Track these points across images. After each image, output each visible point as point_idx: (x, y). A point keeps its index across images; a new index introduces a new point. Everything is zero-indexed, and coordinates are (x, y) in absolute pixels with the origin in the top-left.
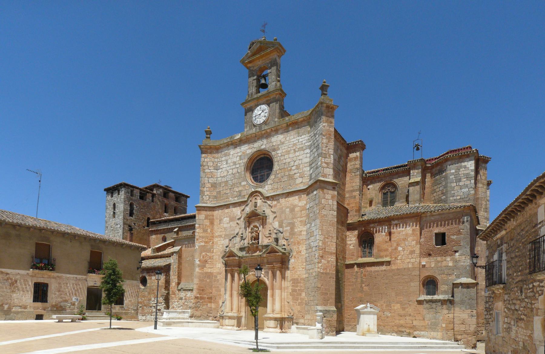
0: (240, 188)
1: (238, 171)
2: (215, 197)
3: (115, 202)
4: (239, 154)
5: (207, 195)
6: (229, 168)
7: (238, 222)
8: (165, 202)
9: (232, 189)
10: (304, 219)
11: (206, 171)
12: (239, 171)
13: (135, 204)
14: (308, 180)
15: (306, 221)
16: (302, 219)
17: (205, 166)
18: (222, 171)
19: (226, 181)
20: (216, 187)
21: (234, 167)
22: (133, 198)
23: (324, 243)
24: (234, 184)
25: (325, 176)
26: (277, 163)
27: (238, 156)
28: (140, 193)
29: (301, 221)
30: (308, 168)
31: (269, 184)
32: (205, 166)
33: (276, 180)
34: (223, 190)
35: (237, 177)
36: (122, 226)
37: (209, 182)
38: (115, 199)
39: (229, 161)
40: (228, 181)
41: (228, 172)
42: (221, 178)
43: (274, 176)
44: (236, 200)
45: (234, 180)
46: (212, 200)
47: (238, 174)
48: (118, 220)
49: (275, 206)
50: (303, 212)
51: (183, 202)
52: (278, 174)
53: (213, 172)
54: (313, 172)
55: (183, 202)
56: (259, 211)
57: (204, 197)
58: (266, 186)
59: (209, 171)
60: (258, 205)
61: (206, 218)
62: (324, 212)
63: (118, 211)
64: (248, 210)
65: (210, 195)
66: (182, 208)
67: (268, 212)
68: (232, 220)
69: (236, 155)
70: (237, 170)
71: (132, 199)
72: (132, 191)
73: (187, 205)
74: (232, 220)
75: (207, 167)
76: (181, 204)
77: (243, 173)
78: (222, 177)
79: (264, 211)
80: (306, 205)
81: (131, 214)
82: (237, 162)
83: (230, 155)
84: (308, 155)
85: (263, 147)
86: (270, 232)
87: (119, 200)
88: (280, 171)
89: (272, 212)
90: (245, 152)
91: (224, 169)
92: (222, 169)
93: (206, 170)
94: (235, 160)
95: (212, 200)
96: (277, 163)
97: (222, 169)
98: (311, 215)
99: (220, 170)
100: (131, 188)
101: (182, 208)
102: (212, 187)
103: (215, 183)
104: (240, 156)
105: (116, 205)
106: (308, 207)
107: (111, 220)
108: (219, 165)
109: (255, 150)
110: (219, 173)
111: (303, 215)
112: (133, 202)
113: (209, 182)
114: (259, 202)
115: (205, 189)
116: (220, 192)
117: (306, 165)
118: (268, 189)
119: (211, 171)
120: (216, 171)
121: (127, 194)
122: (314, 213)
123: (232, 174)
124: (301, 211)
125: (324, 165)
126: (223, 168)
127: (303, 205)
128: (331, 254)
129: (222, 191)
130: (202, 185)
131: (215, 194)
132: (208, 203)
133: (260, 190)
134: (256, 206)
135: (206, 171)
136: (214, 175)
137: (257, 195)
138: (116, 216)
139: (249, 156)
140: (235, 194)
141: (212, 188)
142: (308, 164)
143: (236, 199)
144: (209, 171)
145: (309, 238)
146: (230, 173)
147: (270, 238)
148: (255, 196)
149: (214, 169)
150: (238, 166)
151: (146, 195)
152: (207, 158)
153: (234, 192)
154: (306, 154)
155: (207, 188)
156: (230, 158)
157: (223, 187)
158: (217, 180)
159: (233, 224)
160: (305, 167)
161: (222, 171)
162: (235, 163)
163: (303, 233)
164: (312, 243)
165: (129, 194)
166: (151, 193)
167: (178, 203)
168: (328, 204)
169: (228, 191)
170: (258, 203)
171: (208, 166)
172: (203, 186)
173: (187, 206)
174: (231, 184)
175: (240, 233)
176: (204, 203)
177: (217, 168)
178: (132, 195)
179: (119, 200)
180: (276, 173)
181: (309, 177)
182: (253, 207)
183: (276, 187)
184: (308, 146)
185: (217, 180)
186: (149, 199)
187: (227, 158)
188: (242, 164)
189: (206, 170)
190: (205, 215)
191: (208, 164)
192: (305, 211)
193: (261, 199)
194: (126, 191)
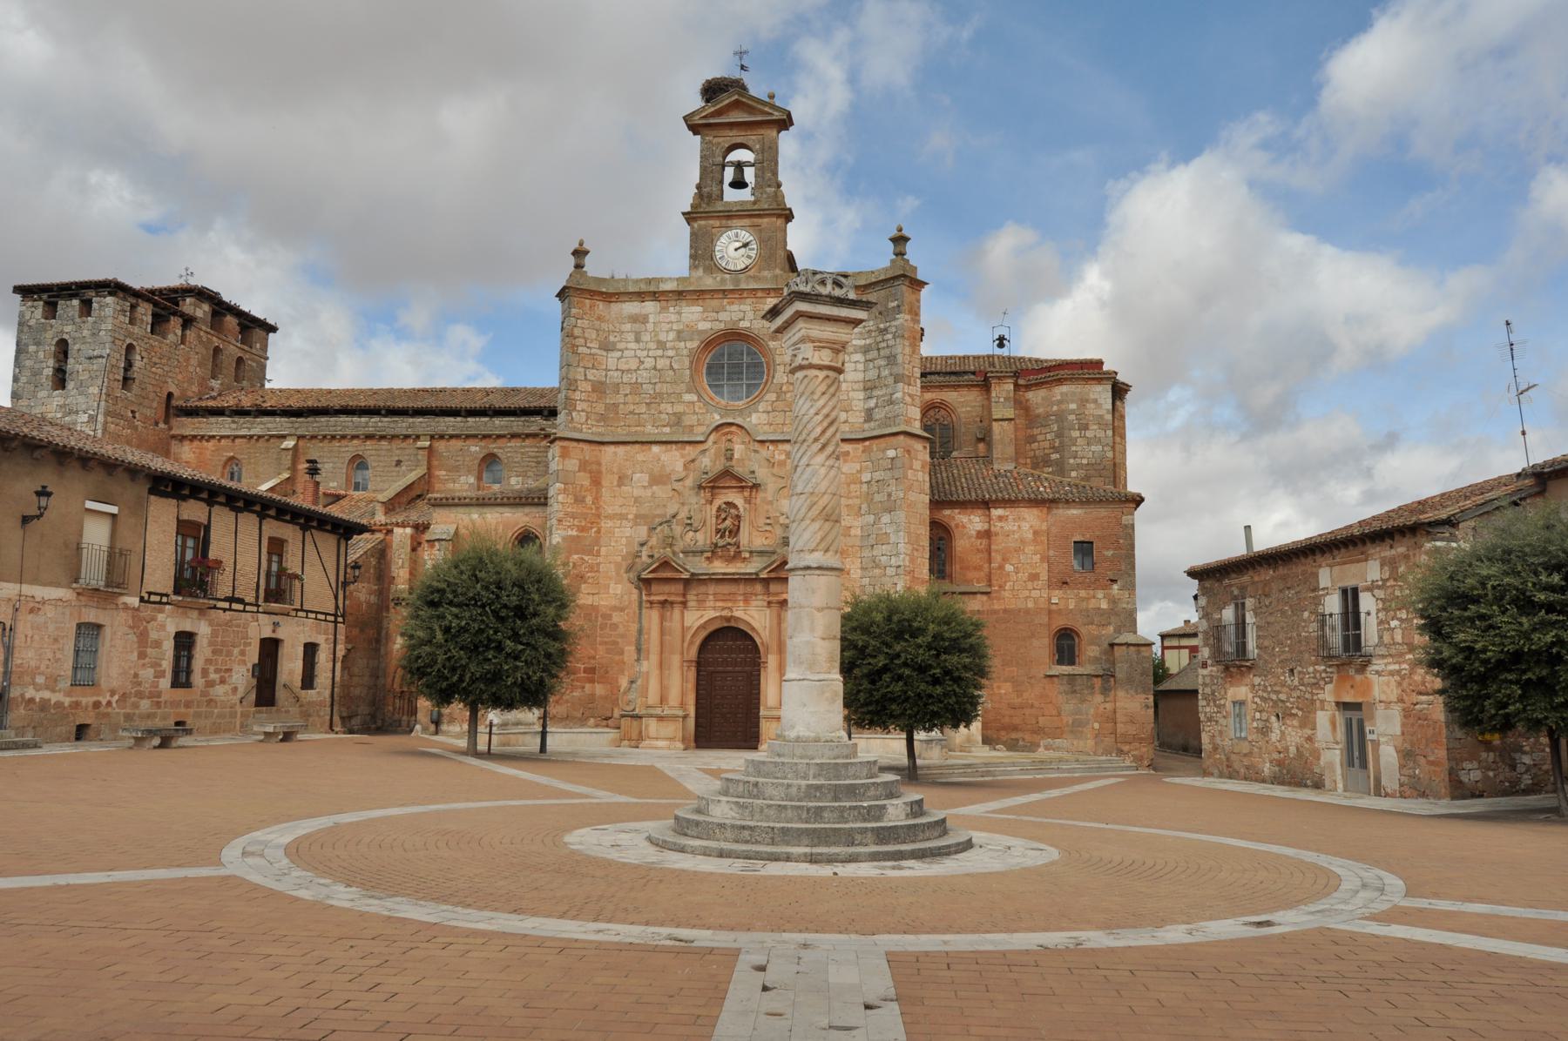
0: (679, 408)
1: (671, 366)
2: (602, 418)
3: (66, 337)
4: (674, 328)
5: (583, 411)
6: (645, 353)
7: (677, 486)
8: (213, 342)
9: (653, 405)
10: (857, 501)
11: (581, 350)
12: (675, 366)
13: (137, 348)
14: (862, 420)
15: (860, 508)
16: (850, 502)
17: (578, 337)
18: (622, 357)
19: (636, 383)
20: (605, 392)
21: (660, 352)
22: (136, 330)
23: (912, 560)
24: (660, 394)
25: (908, 422)
26: (782, 367)
27: (672, 330)
28: (154, 315)
29: (847, 506)
30: (861, 395)
31: (761, 410)
32: (578, 337)
33: (780, 405)
34: (624, 404)
35: (668, 379)
36: (101, 418)
37: (586, 379)
38: (68, 329)
39: (646, 337)
40: (642, 384)
41: (643, 363)
42: (619, 373)
43: (775, 395)
44: (666, 432)
45: (658, 387)
46: (594, 423)
47: (671, 373)
48: (81, 399)
49: (782, 464)
50: (852, 486)
51: (258, 345)
52: (785, 393)
53: (596, 354)
54: (876, 406)
55: (258, 345)
56: (739, 470)
57: (574, 414)
58: (754, 416)
59: (588, 351)
60: (736, 456)
61: (584, 466)
62: (913, 496)
63: (80, 368)
64: (709, 462)
65: (589, 410)
66: (254, 364)
67: (762, 474)
68: (658, 479)
69: (666, 327)
70: (668, 363)
71: (130, 335)
72: (133, 307)
73: (269, 354)
74: (658, 479)
75: (581, 341)
76: (254, 351)
77: (688, 372)
78: (623, 372)
79: (753, 472)
80: (860, 472)
81: (127, 381)
82: (669, 345)
83: (648, 322)
84: (860, 367)
85: (744, 324)
86: (768, 521)
87: (86, 333)
88: (791, 388)
89: (774, 475)
90: (692, 324)
91: (626, 353)
92: (622, 351)
93: (580, 349)
94: (662, 337)
95: (594, 423)
96: (782, 367)
97: (622, 351)
98: (877, 498)
99: (619, 354)
100: (134, 301)
101: (254, 364)
102: (594, 390)
103: (602, 383)
104: (679, 332)
105: (73, 348)
106: (866, 477)
107: (42, 394)
108: (612, 338)
109: (722, 326)
110: (612, 359)
111: (853, 494)
112: (134, 343)
113: (586, 379)
114: (739, 450)
115: (577, 395)
116: (616, 405)
117: (856, 386)
118: (759, 422)
119: (593, 351)
120: (605, 353)
121: (122, 318)
122: (889, 495)
123: (655, 368)
124: (849, 485)
125: (908, 399)
126: (627, 349)
127: (855, 472)
128: (923, 582)
129: (621, 406)
130: (570, 385)
131: (600, 408)
132: (584, 430)
133: (739, 421)
134: (730, 459)
135: (581, 350)
136: (599, 363)
137: (731, 433)
138: (70, 385)
139: (704, 337)
140: (664, 420)
141: (595, 395)
142: (861, 385)
143: (667, 430)
144: (588, 351)
145: (873, 546)
146: (647, 365)
147: (767, 535)
148: (727, 434)
149: (600, 348)
150: (671, 353)
151: (168, 321)
152: (582, 319)
153: (660, 412)
154: (855, 362)
155: (582, 392)
156: (646, 330)
157: (626, 395)
158: (606, 376)
159: (661, 492)
160: (853, 390)
161: (622, 357)
162: (661, 345)
163: (853, 532)
164: (884, 559)
165: (125, 316)
166: (180, 316)
167: (246, 348)
168: (917, 481)
169: (643, 409)
170: (736, 450)
171: (586, 339)
172: (573, 388)
173: (267, 359)
174: (652, 392)
175: (683, 515)
176: (575, 429)
177: (607, 347)
178: (132, 321)
179: (86, 333)
180: (781, 389)
181: (863, 414)
182: (723, 459)
183: (780, 420)
184: (861, 347)
185: (606, 376)
186: (176, 335)
187: (637, 326)
188: (685, 352)
189: (580, 349)
190: (580, 460)
191: (586, 335)
192: (858, 486)
193: (743, 443)
194: (119, 308)
